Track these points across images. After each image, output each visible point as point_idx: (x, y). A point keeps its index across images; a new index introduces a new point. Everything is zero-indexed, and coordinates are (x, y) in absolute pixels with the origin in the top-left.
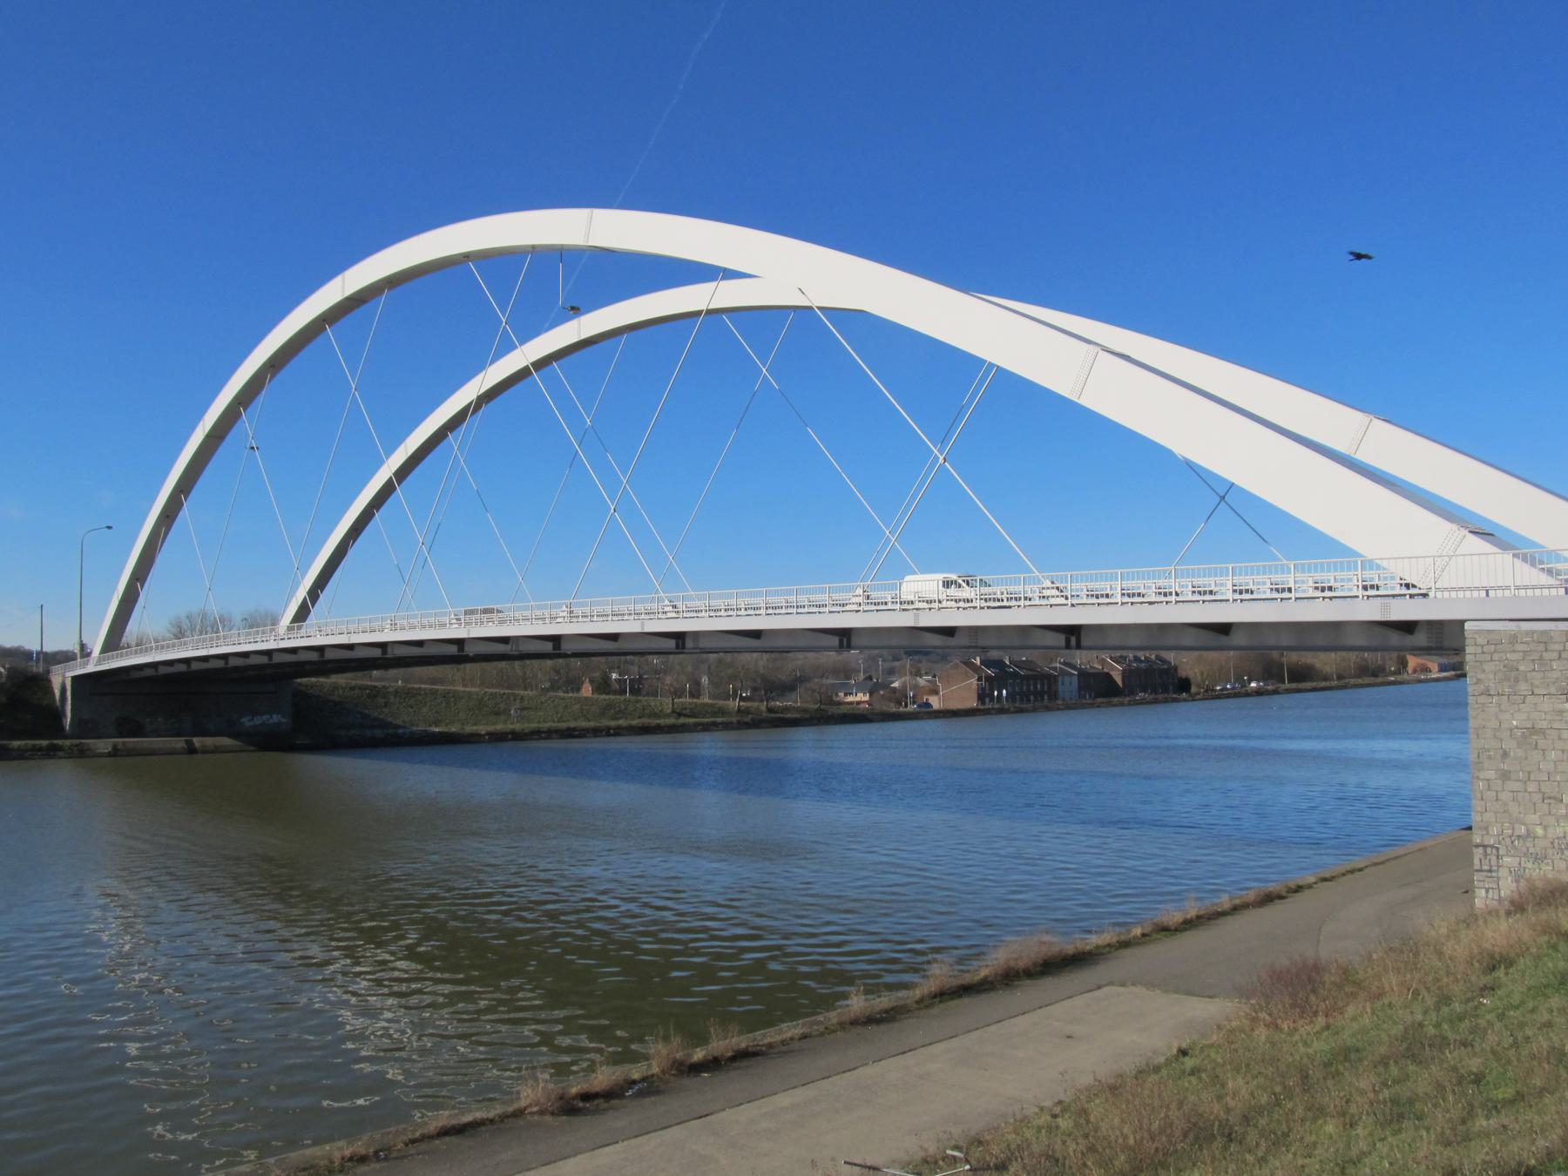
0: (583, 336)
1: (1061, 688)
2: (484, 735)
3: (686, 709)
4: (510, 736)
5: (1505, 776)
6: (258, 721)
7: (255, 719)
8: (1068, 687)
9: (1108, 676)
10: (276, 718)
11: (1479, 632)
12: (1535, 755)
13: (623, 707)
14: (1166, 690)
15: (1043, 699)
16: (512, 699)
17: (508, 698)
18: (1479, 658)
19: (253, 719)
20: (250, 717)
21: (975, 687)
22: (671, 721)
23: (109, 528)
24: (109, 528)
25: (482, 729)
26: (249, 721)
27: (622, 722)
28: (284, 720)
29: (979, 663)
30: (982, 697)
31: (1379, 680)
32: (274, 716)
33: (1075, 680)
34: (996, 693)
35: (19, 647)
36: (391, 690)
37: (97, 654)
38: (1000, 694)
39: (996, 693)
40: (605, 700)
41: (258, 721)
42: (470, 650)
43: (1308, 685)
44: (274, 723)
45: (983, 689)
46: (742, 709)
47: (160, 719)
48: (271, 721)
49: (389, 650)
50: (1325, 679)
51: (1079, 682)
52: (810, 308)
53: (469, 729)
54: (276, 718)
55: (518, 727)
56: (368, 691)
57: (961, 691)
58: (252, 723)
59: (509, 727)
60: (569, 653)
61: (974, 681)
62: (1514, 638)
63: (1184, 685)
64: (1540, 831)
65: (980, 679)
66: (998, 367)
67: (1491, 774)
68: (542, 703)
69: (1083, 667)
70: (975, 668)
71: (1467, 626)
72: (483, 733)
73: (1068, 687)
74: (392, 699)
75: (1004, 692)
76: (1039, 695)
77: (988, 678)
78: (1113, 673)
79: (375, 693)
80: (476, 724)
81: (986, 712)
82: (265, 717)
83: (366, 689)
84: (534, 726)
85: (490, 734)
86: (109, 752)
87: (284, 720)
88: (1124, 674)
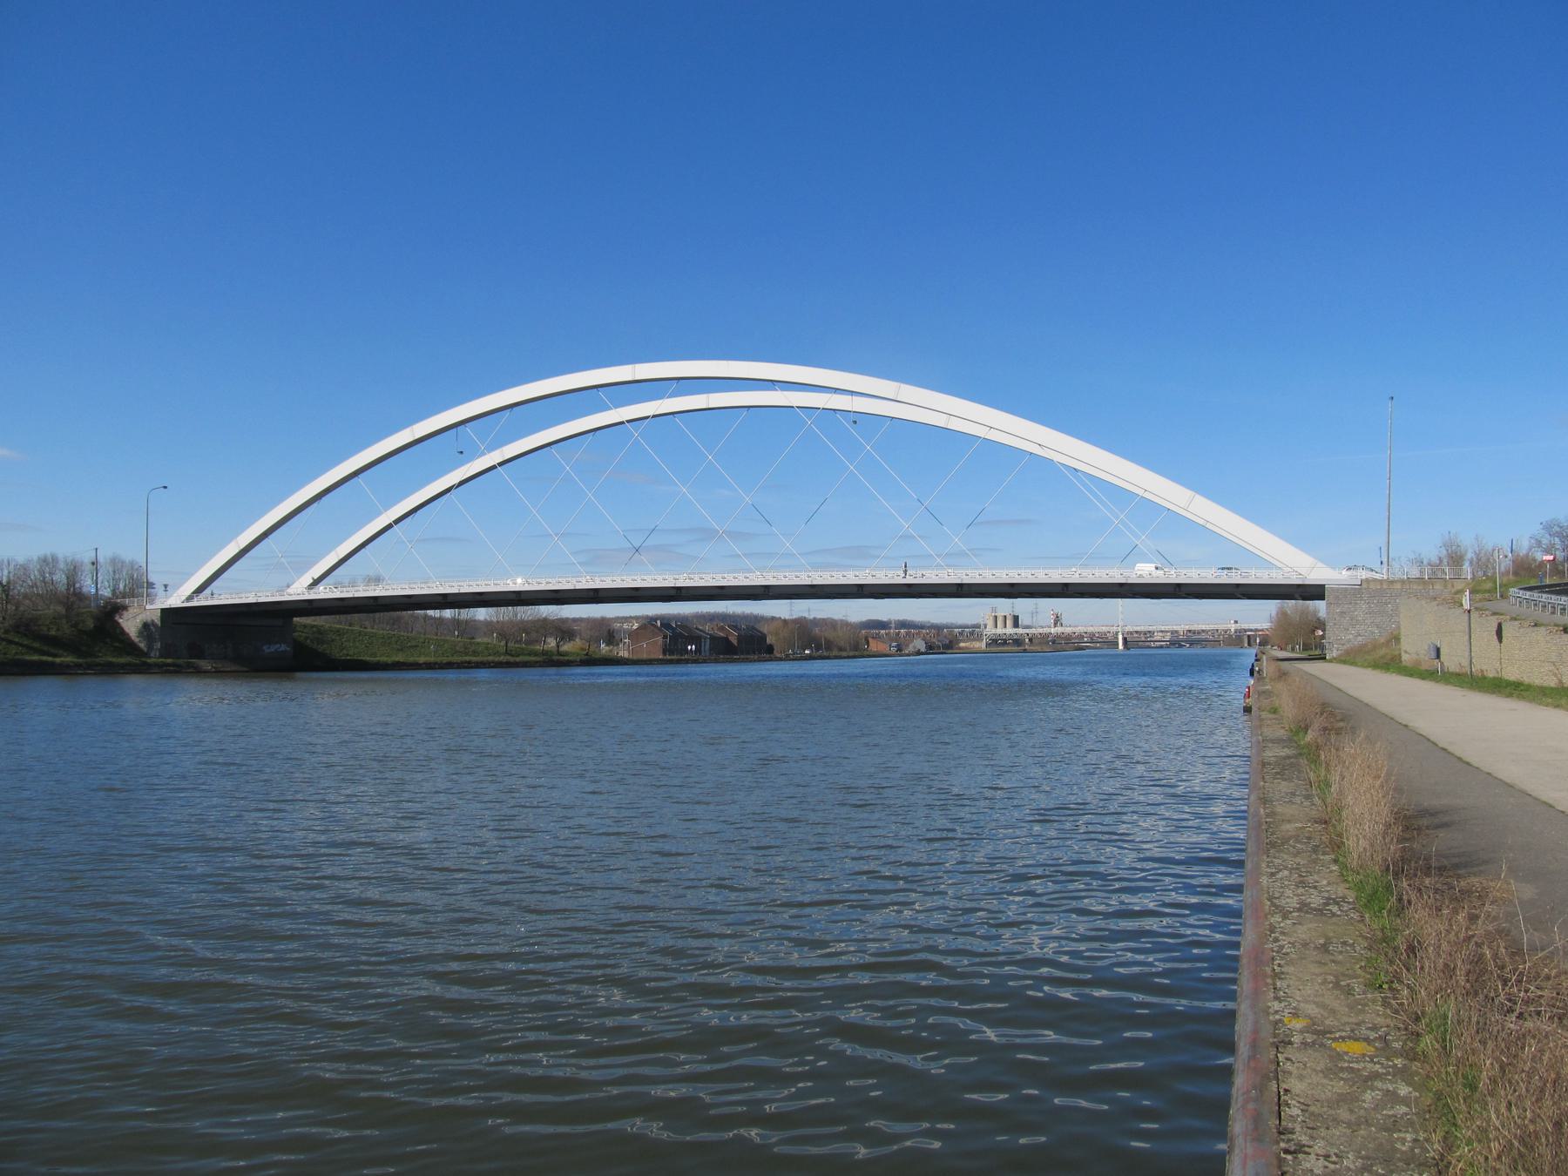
6: (273, 648)
9: (726, 640)
10: (283, 647)
20: (268, 646)
23: (165, 487)
24: (165, 487)
28: (288, 649)
30: (664, 654)
34: (689, 647)
41: (273, 648)
50: (841, 649)
53: (411, 659)
54: (283, 647)
61: (660, 639)
62: (1338, 589)
63: (770, 649)
65: (665, 637)
72: (421, 662)
78: (730, 638)
79: (320, 631)
87: (288, 649)
88: (739, 638)
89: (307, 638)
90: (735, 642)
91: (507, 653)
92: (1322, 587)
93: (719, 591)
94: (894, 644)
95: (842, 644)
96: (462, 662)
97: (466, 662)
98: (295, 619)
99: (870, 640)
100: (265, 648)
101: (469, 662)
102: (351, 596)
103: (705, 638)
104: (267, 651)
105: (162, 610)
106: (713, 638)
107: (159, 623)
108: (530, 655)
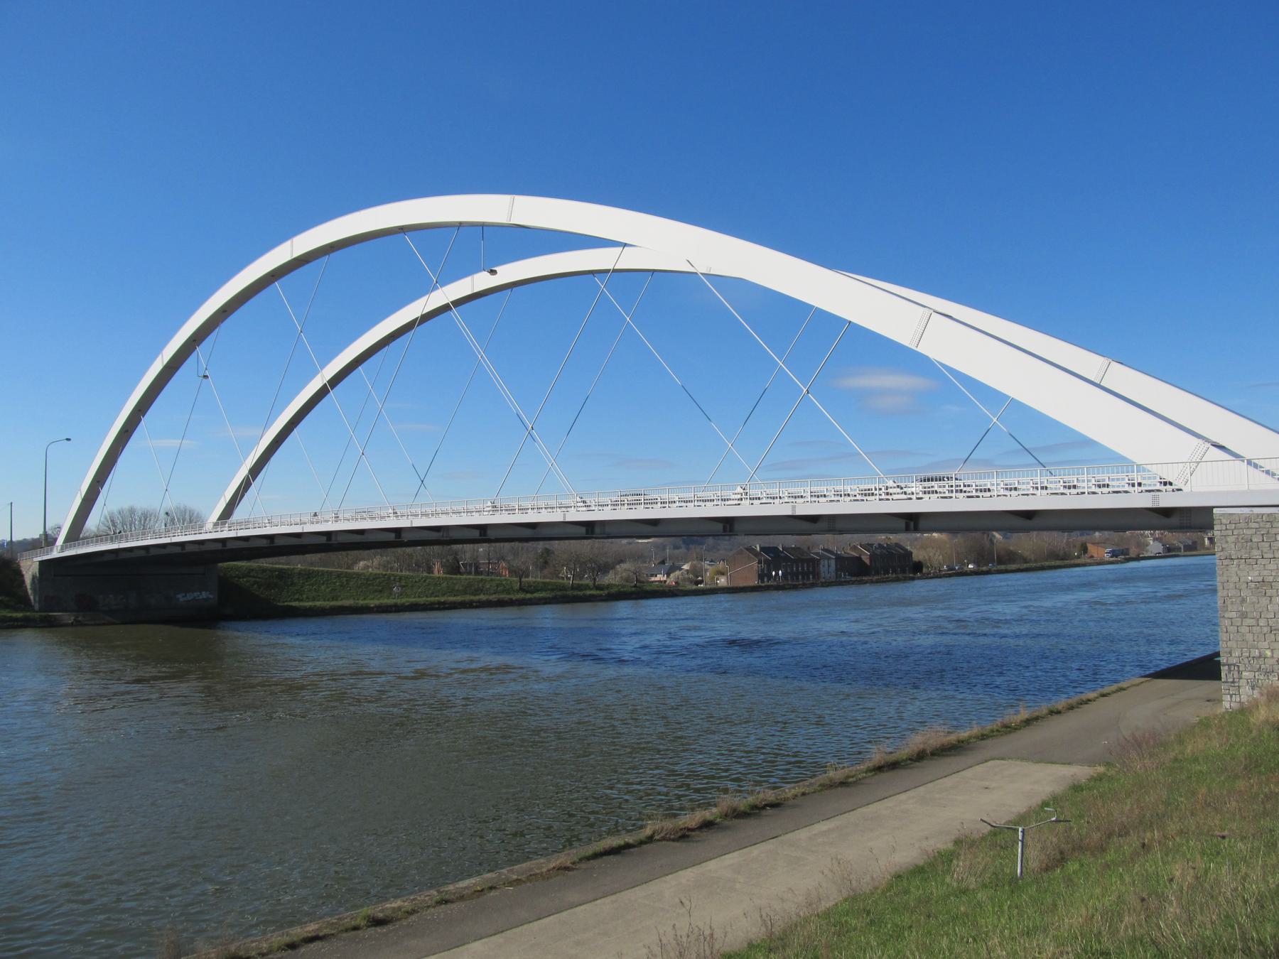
0: (476, 290)
1: (822, 569)
2: (373, 608)
3: (531, 586)
4: (394, 608)
5: (1244, 616)
6: (190, 597)
7: (188, 595)
8: (828, 569)
9: (859, 559)
10: (204, 595)
11: (1223, 515)
12: (1264, 601)
13: (480, 585)
14: (904, 571)
15: (808, 578)
16: (392, 578)
17: (389, 578)
18: (1224, 533)
19: (186, 596)
20: (184, 595)
21: (755, 568)
22: (521, 596)
25: (373, 603)
26: (183, 597)
27: (483, 597)
28: (211, 596)
29: (758, 549)
30: (761, 577)
31: (1066, 562)
32: (204, 593)
33: (833, 563)
34: (774, 573)
35: (25, 539)
36: (295, 571)
37: (61, 544)
38: (777, 574)
39: (774, 573)
40: (466, 579)
41: (190, 597)
42: (406, 537)
43: (1014, 567)
44: (204, 599)
45: (763, 570)
46: (575, 586)
47: (111, 596)
48: (201, 597)
49: (333, 538)
50: (1026, 561)
51: (836, 566)
52: (696, 273)
53: (361, 602)
54: (204, 595)
55: (399, 601)
56: (277, 573)
57: (748, 573)
58: (185, 599)
59: (390, 601)
60: (493, 538)
61: (755, 563)
62: (1248, 519)
64: (1268, 653)
65: (760, 562)
66: (850, 322)
67: (1234, 615)
68: (416, 582)
69: (839, 553)
70: (756, 554)
71: (1215, 510)
72: (372, 605)
73: (828, 569)
74: (296, 580)
75: (780, 572)
76: (805, 575)
77: (766, 561)
78: (863, 557)
79: (283, 575)
80: (365, 599)
81: (768, 588)
82: (196, 594)
83: (275, 571)
84: (413, 600)
85: (376, 606)
86: (72, 623)
87: (211, 596)
88: (871, 558)
89: (255, 582)
90: (867, 562)
91: (522, 589)
92: (1208, 510)
93: (358, 538)
94: (1108, 550)
95: (1026, 554)
96: (433, 603)
97: (439, 603)
98: (220, 564)
99: (1089, 546)
100: (179, 596)
101: (444, 603)
102: (117, 547)
103: (829, 558)
104: (181, 600)
105: (40, 562)
106: (839, 559)
107: (38, 575)
108: (552, 590)
